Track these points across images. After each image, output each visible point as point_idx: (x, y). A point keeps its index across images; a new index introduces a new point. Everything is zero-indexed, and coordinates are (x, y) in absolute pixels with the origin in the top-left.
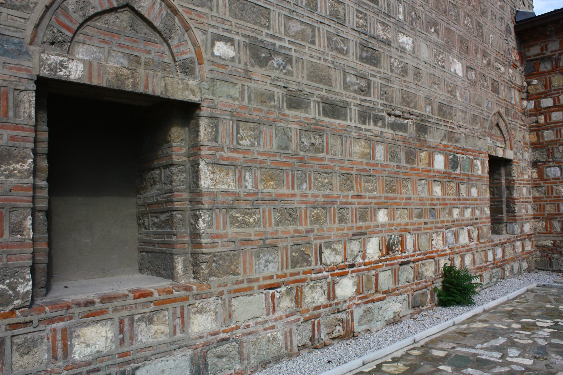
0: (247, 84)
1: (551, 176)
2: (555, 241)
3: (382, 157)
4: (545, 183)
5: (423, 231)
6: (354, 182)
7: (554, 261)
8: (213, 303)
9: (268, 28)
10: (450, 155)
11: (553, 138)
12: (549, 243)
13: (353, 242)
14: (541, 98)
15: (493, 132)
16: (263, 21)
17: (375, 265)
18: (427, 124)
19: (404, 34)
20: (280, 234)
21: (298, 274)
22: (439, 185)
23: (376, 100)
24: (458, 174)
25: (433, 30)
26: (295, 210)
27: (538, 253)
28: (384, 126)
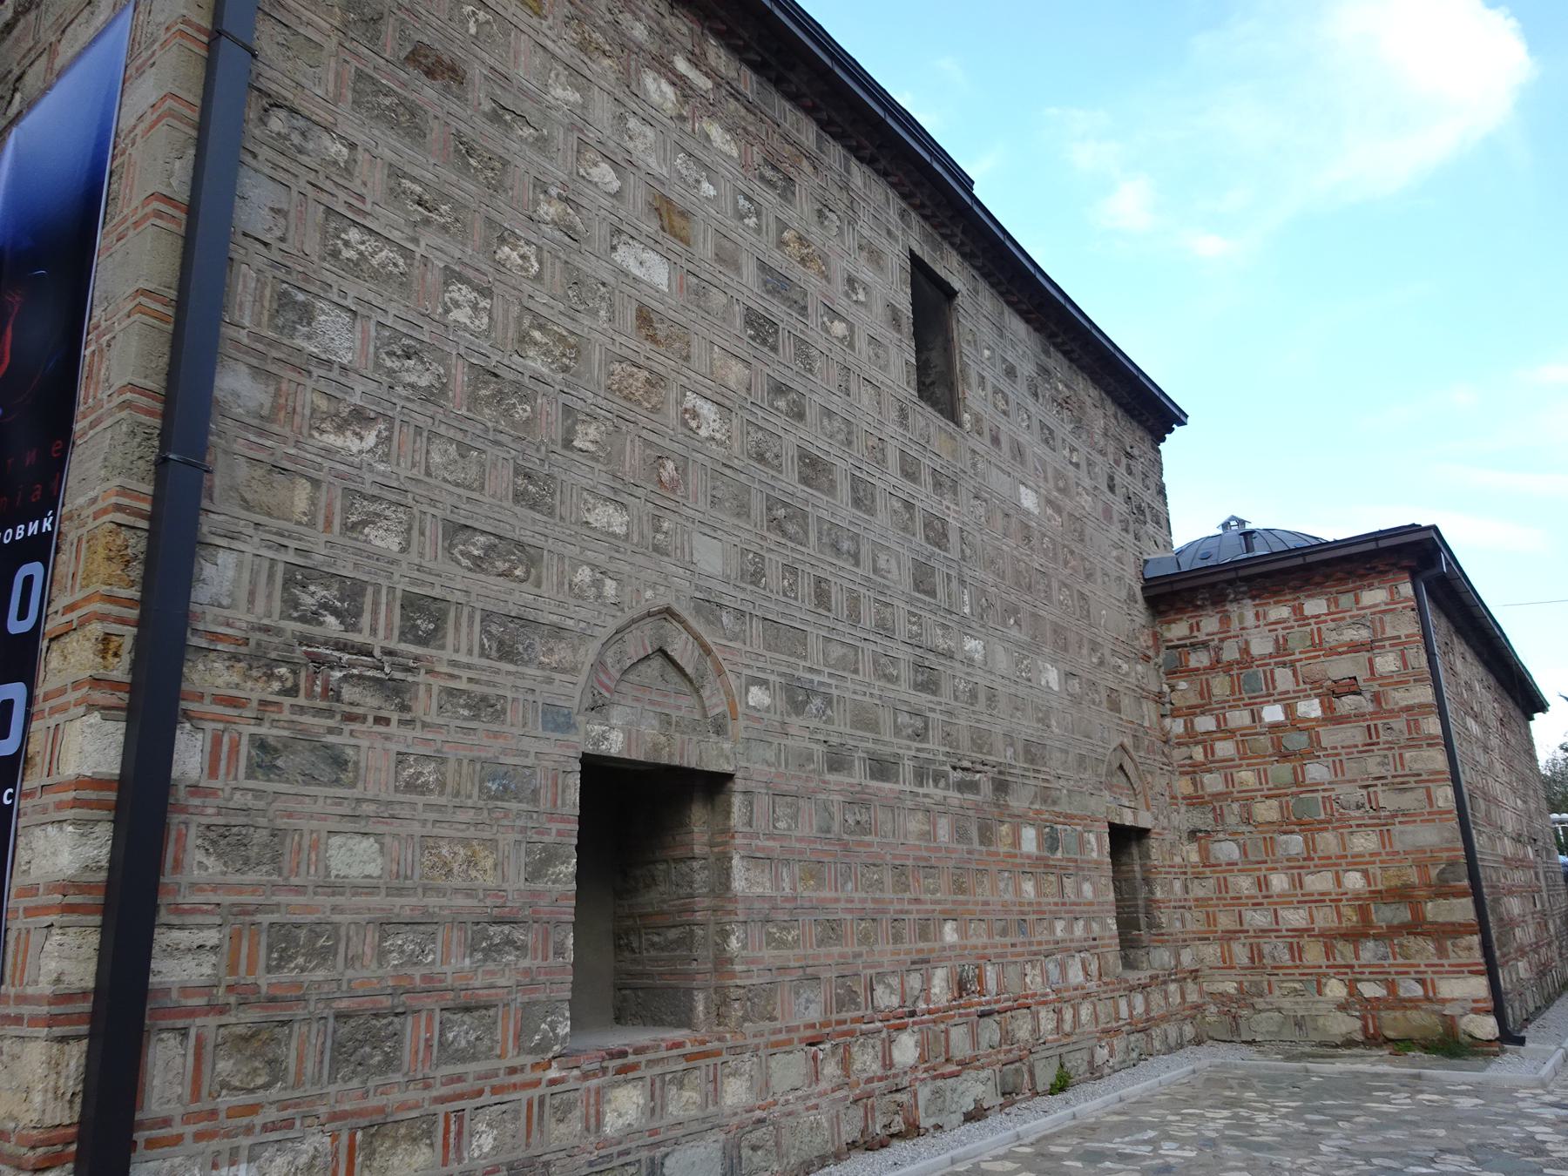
0: (784, 742)
1: (1223, 859)
2: (1241, 983)
4: (1215, 872)
5: (1010, 959)
7: (1242, 1022)
8: (747, 1064)
9: (805, 658)
11: (1221, 788)
12: (1230, 987)
14: (1195, 714)
15: (1115, 781)
16: (800, 649)
17: (940, 1015)
18: (1009, 778)
19: (972, 636)
20: (822, 961)
21: (844, 1022)
23: (936, 747)
24: (1059, 860)
25: (1012, 621)
26: (839, 922)
27: (1213, 1009)
28: (947, 787)
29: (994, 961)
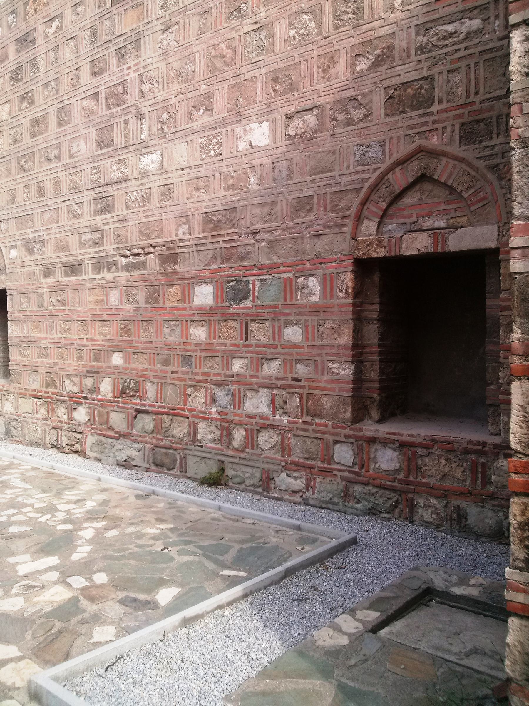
3: (117, 301)
5: (169, 381)
6: (89, 328)
13: (88, 378)
17: (105, 403)
18: (179, 251)
20: (39, 364)
21: (48, 393)
22: (203, 326)
23: (109, 247)
24: (245, 308)
28: (118, 270)
29: (152, 379)
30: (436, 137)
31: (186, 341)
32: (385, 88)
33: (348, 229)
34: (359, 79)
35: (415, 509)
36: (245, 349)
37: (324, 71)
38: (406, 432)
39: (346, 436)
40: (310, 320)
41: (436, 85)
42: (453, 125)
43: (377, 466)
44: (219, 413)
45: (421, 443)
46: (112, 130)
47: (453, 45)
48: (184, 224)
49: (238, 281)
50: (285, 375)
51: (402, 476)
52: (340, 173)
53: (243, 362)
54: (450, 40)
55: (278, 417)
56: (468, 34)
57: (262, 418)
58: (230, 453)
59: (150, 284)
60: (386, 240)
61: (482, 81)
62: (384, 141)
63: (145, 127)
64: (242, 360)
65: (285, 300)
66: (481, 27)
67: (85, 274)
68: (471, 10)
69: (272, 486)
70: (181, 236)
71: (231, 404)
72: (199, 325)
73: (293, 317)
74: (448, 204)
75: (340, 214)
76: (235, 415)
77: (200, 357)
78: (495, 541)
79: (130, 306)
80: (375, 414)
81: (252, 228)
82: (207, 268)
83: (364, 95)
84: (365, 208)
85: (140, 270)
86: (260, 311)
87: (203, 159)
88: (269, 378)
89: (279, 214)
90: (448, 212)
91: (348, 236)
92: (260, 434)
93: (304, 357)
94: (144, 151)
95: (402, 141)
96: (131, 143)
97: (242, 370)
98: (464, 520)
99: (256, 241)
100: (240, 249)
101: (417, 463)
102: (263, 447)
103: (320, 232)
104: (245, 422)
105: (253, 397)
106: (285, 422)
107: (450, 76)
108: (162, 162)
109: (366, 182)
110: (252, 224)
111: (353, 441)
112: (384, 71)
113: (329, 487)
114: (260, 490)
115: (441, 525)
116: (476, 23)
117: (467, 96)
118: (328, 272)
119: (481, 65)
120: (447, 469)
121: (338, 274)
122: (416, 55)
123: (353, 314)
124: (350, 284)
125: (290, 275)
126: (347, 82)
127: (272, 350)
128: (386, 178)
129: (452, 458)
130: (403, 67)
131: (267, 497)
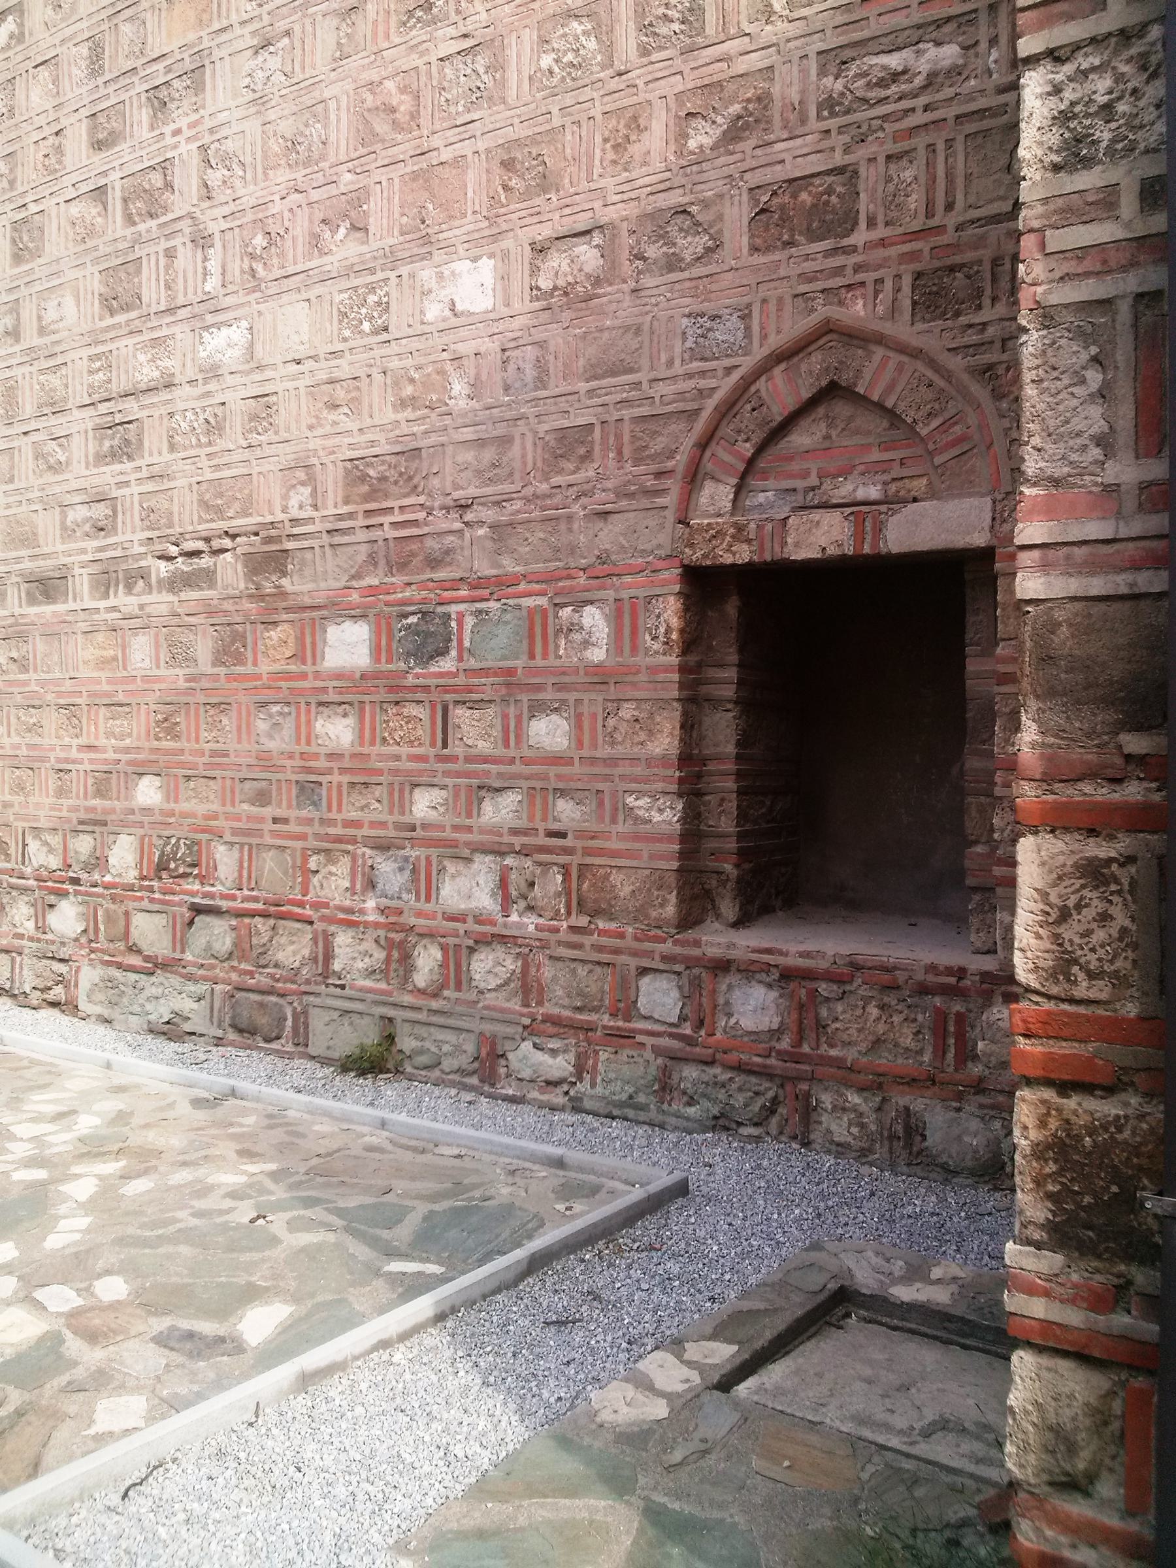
3: (148, 660)
5: (268, 840)
6: (84, 721)
10: (405, 616)
13: (82, 837)
17: (119, 892)
18: (290, 545)
22: (345, 715)
23: (129, 537)
24: (441, 675)
29: (228, 837)
30: (860, 302)
31: (306, 749)
32: (751, 189)
33: (669, 500)
34: (694, 168)
35: (814, 1116)
36: (440, 766)
37: (616, 147)
38: (793, 948)
39: (665, 958)
40: (586, 702)
41: (861, 187)
42: (898, 276)
43: (733, 1021)
44: (382, 911)
45: (827, 971)
46: (139, 271)
47: (900, 99)
48: (303, 484)
49: (424, 614)
50: (531, 825)
51: (785, 1044)
52: (653, 375)
53: (437, 796)
54: (894, 88)
55: (514, 917)
56: (932, 76)
57: (479, 920)
58: (408, 999)
59: (224, 620)
60: (753, 526)
61: (960, 182)
62: (749, 306)
63: (214, 265)
64: (436, 792)
65: (532, 656)
66: (961, 62)
67: (75, 599)
68: (939, 24)
69: (502, 1071)
70: (295, 513)
71: (409, 891)
72: (336, 714)
73: (548, 695)
74: (886, 450)
75: (653, 468)
76: (420, 914)
77: (340, 786)
78: (986, 1182)
79: (177, 671)
80: (729, 908)
81: (457, 494)
82: (355, 584)
83: (705, 204)
84: (708, 453)
85: (202, 589)
86: (476, 681)
87: (345, 340)
88: (495, 831)
89: (517, 465)
90: (885, 466)
91: (670, 516)
92: (476, 956)
93: (572, 785)
94: (210, 319)
95: (788, 307)
96: (181, 300)
97: (434, 813)
98: (919, 1138)
99: (466, 524)
100: (429, 543)
101: (817, 1015)
102: (482, 985)
103: (609, 507)
104: (442, 931)
105: (459, 874)
106: (531, 928)
107: (892, 166)
108: (251, 345)
109: (710, 396)
110: (458, 488)
111: (678, 967)
112: (749, 151)
113: (626, 1071)
114: (474, 1080)
115: (870, 1151)
116: (949, 54)
117: (929, 214)
118: (625, 594)
119: (959, 146)
120: (881, 1028)
121: (649, 599)
122: (819, 117)
123: (681, 689)
124: (675, 622)
125: (542, 601)
126: (668, 175)
127: (503, 768)
128: (753, 389)
129: (894, 1002)
130: (791, 143)
131: (489, 1096)
